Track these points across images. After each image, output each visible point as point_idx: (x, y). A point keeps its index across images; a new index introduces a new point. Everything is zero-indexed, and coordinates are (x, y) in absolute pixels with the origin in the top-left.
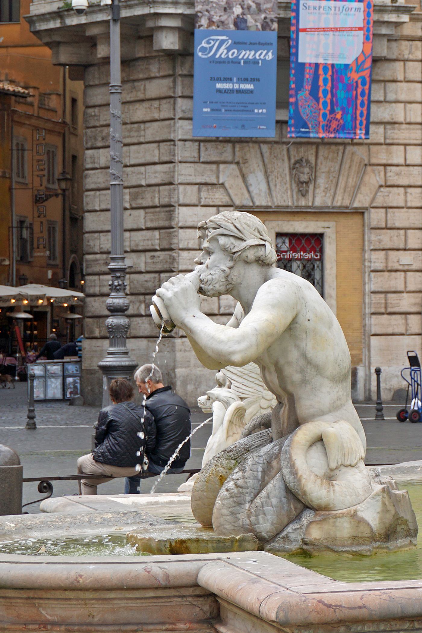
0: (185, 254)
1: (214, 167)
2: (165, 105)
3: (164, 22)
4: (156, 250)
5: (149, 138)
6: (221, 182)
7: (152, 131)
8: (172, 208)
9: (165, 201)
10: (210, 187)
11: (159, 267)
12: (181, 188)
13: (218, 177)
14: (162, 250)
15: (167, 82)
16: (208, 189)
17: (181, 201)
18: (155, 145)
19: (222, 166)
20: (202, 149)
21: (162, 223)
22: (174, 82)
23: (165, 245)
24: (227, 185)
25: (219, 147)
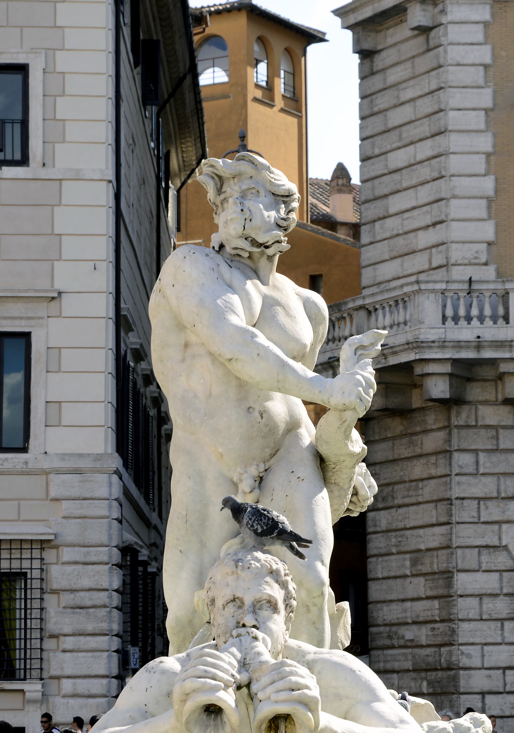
0: (465, 626)
1: (496, 527)
2: (442, 460)
3: (431, 368)
4: (435, 621)
5: (427, 498)
6: (504, 544)
7: (429, 490)
8: (450, 575)
9: (443, 566)
10: (492, 550)
11: (439, 640)
12: (459, 552)
13: (500, 539)
14: (442, 621)
15: (441, 435)
16: (490, 553)
17: (460, 567)
18: (432, 505)
19: (504, 527)
20: (482, 507)
21: (441, 591)
22: (450, 434)
23: (445, 616)
24: (510, 547)
25: (502, 505)
